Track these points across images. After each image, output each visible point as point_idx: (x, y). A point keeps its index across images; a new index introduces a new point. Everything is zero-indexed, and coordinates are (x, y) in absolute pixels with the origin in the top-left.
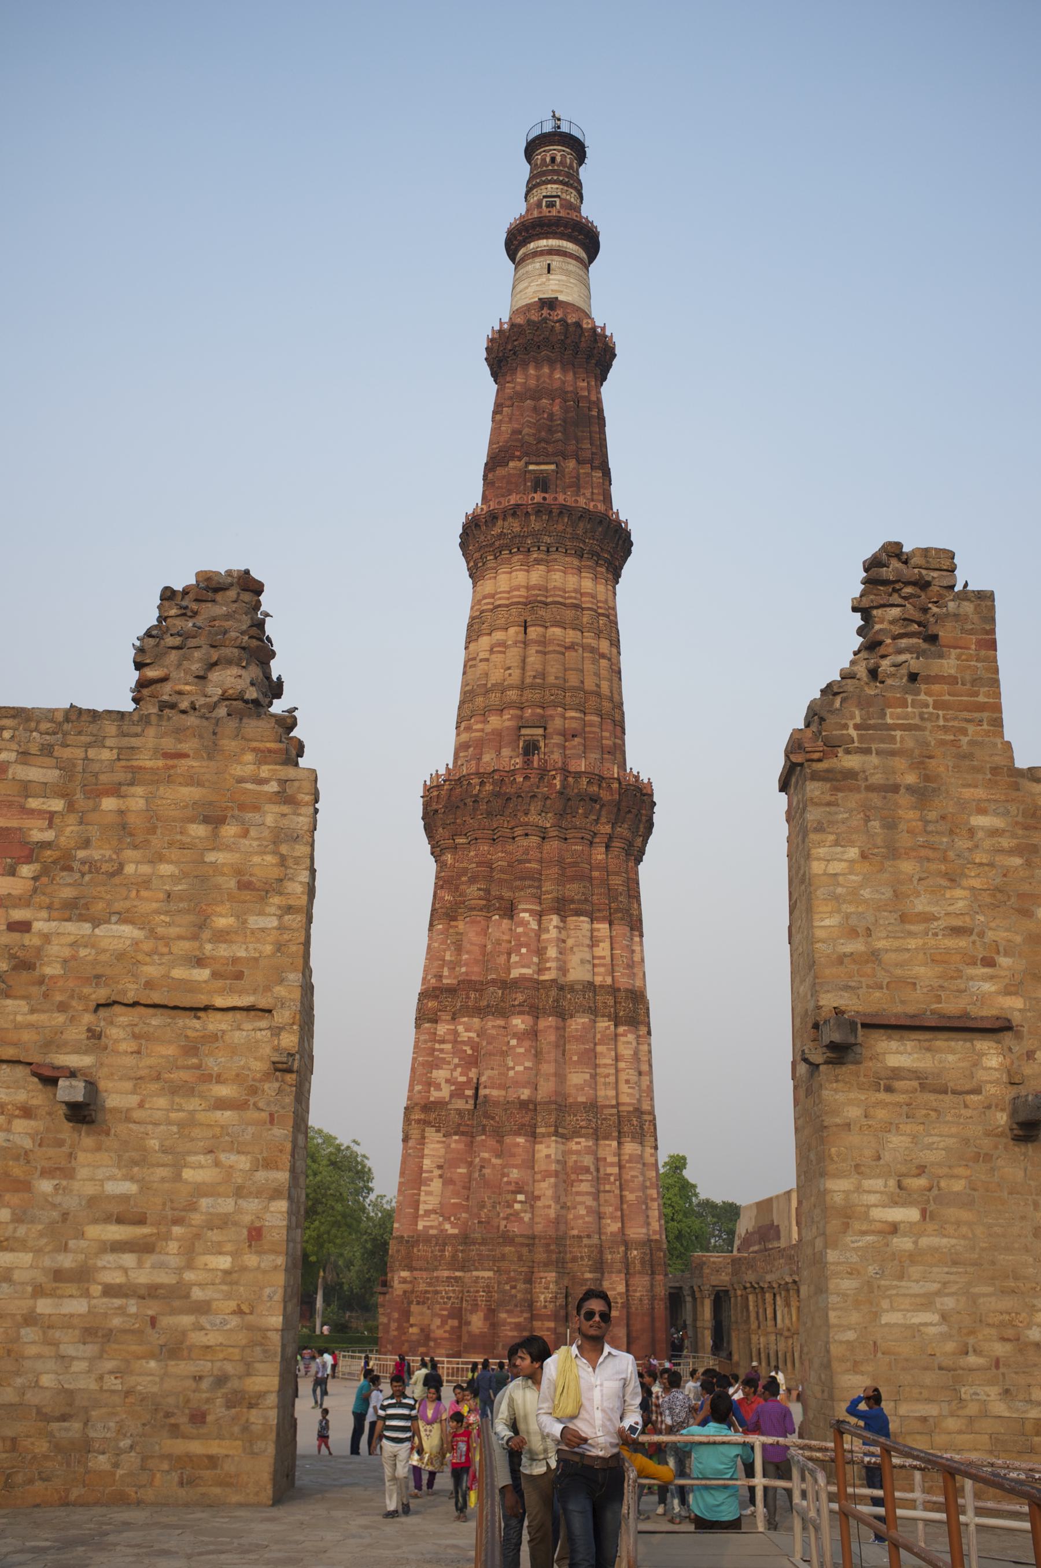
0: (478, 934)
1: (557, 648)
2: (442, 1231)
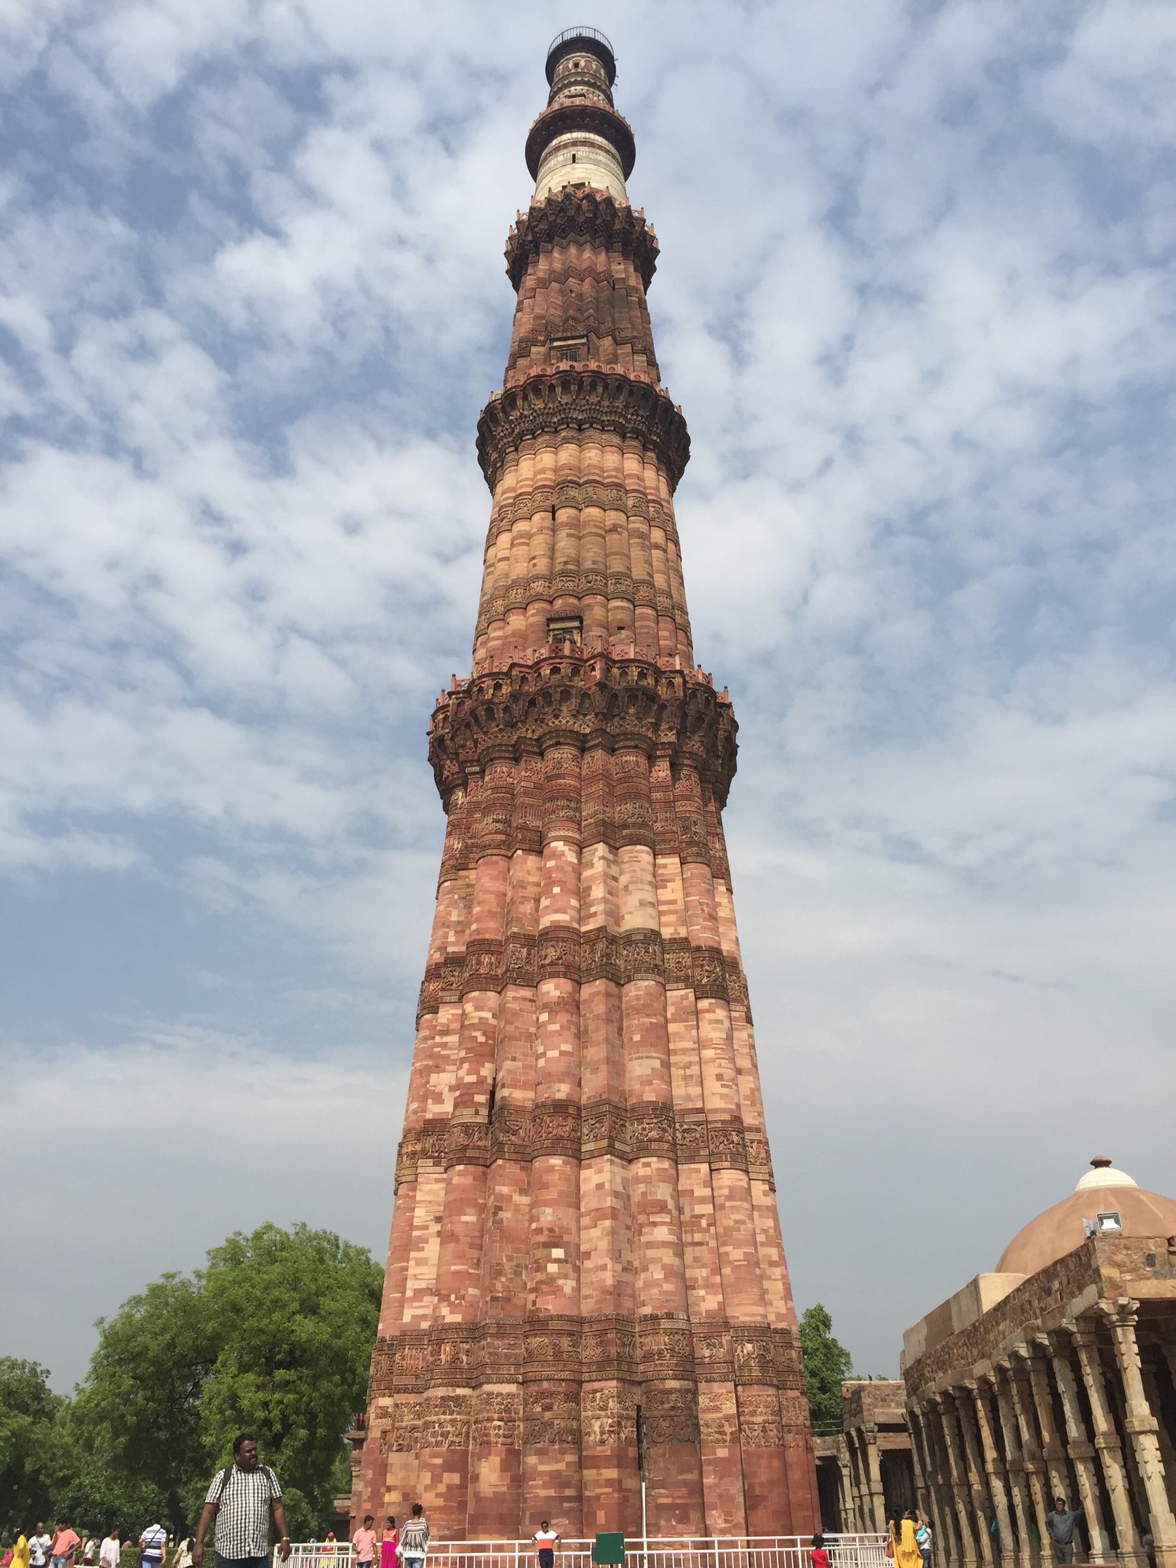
0: (493, 878)
1: (594, 530)
2: (436, 1319)
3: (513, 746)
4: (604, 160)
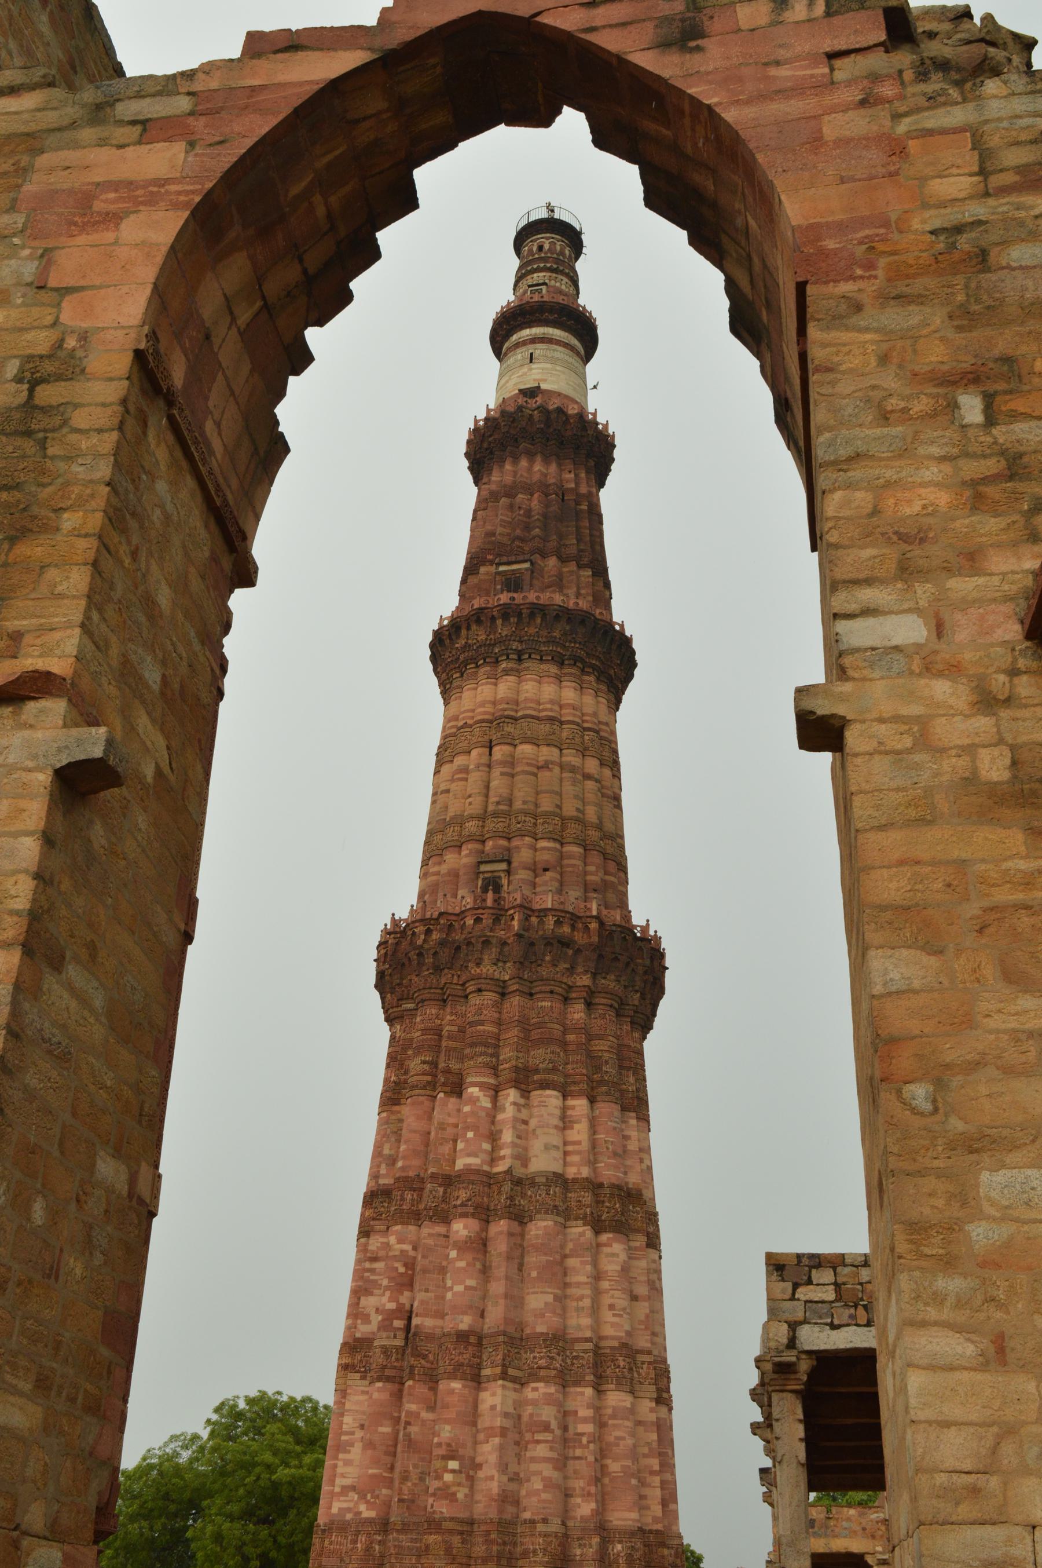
3: (442, 989)
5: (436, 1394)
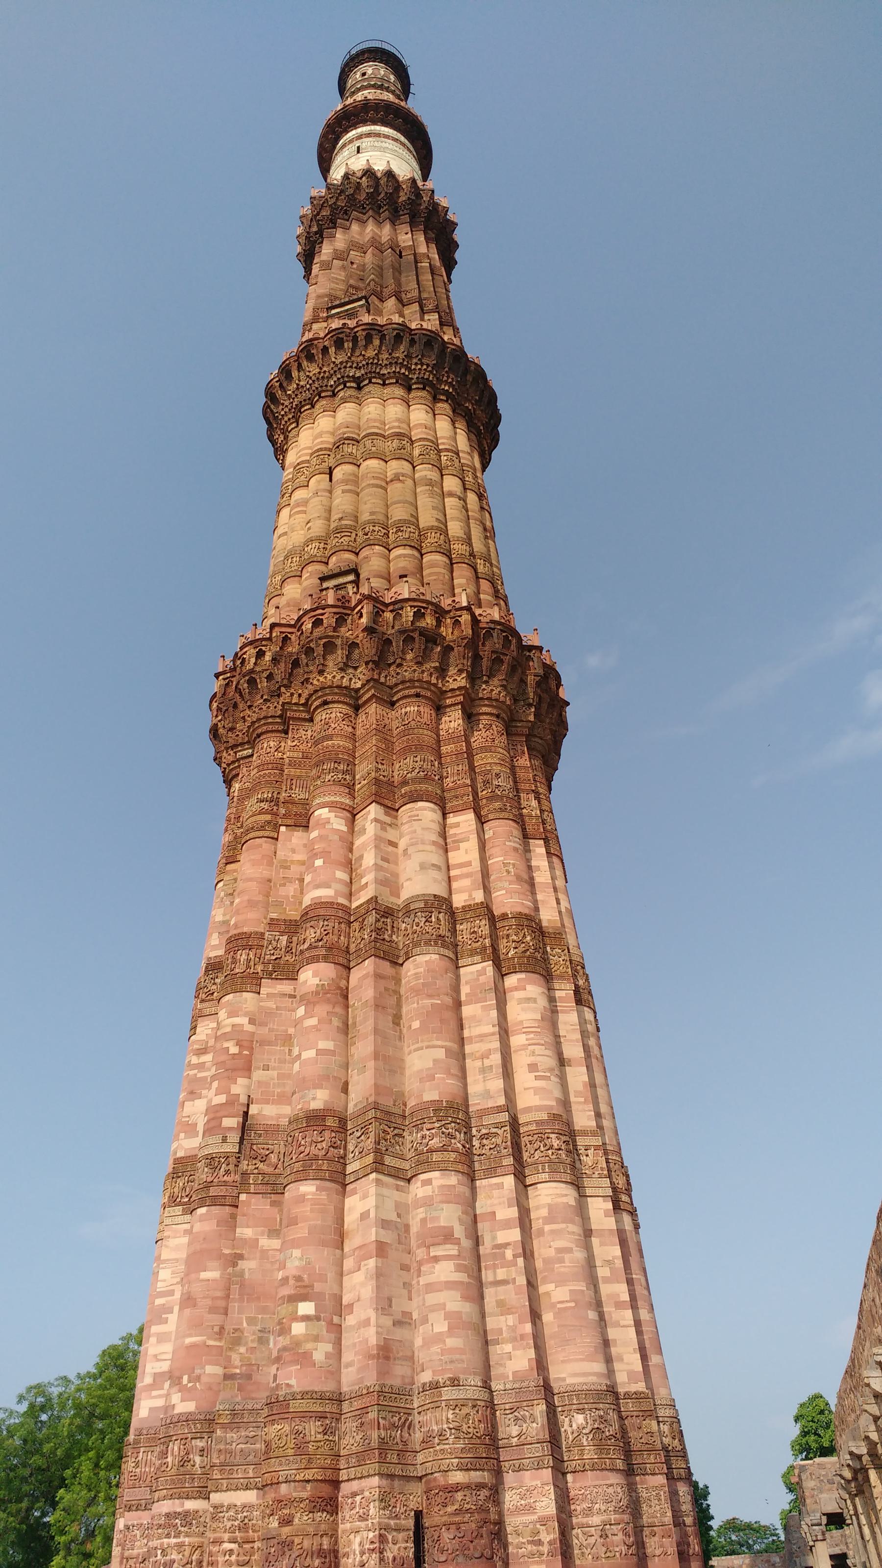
3: (280, 716)
4: (390, 147)
5: (281, 1211)
